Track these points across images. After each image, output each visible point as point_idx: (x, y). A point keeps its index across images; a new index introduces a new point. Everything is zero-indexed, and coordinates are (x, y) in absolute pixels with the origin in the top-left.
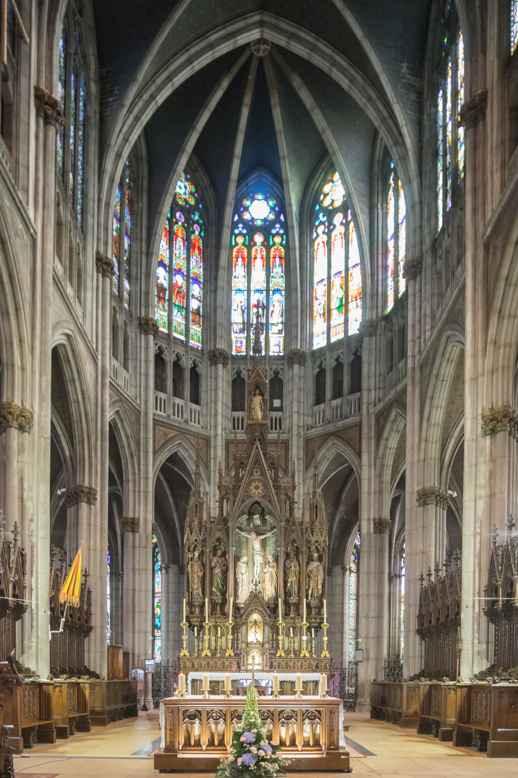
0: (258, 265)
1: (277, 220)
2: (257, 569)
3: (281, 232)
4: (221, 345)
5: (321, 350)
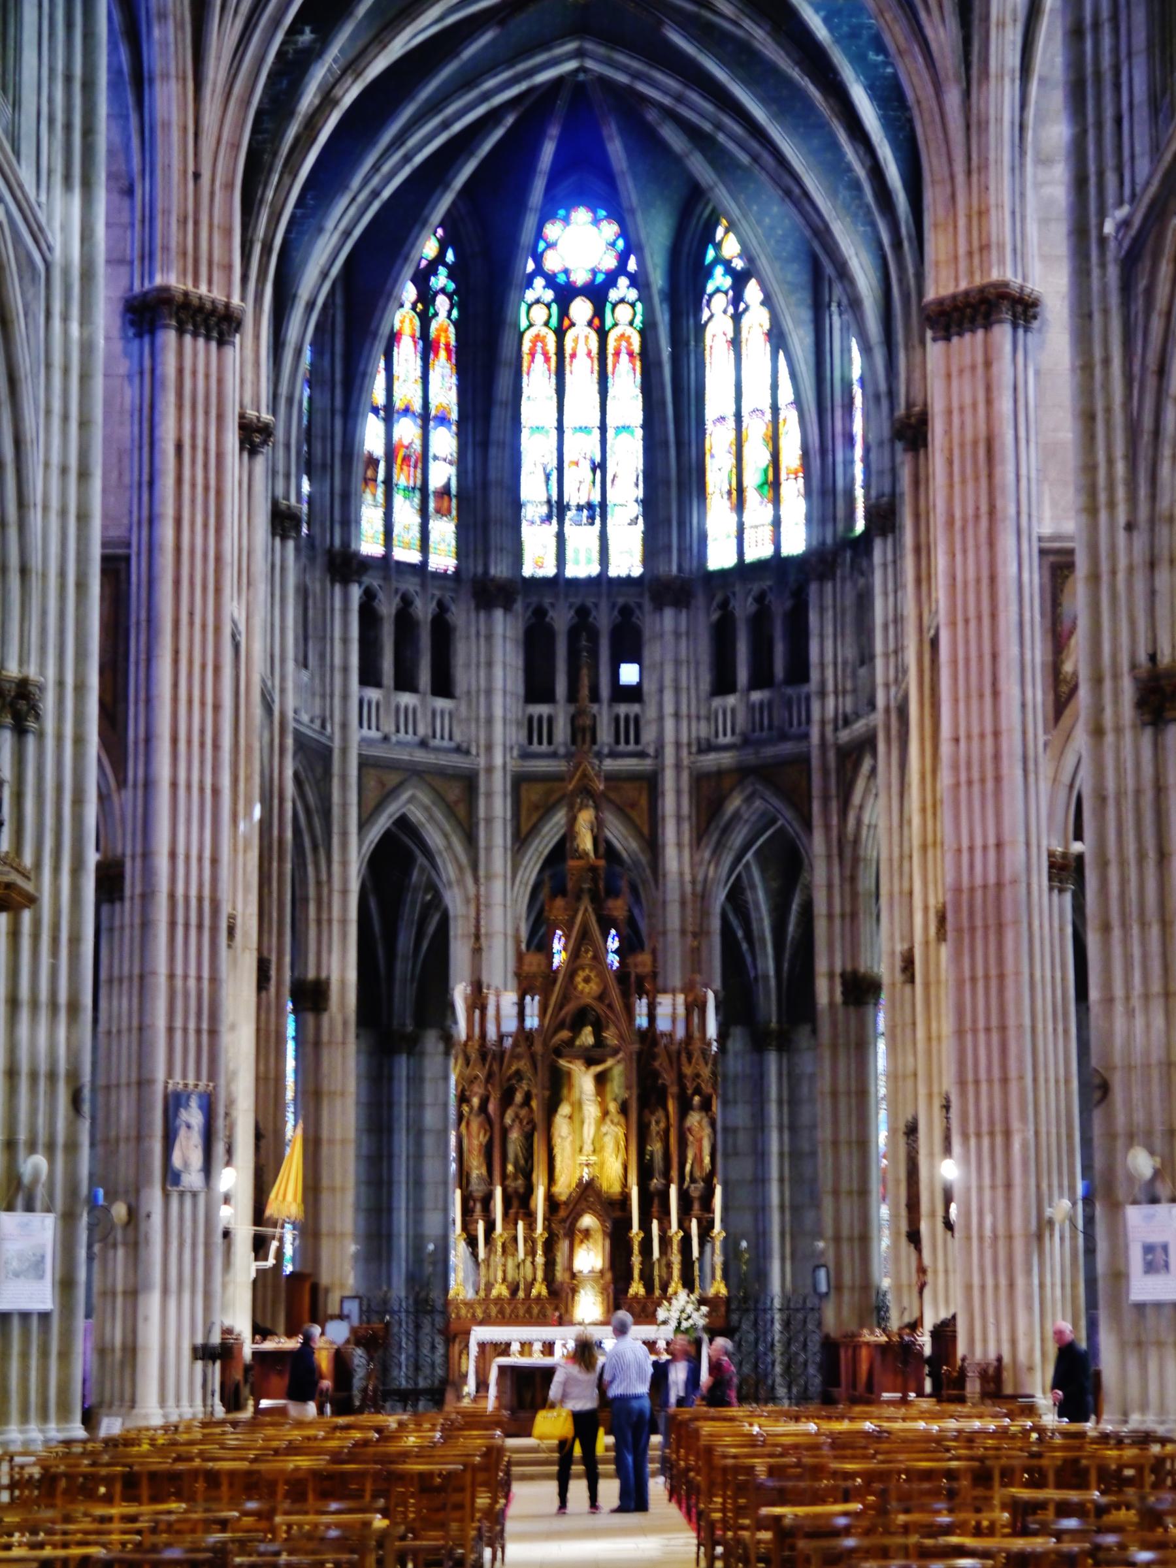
0: (582, 375)
1: (621, 269)
2: (589, 1131)
3: (632, 294)
4: (499, 570)
5: (723, 574)
